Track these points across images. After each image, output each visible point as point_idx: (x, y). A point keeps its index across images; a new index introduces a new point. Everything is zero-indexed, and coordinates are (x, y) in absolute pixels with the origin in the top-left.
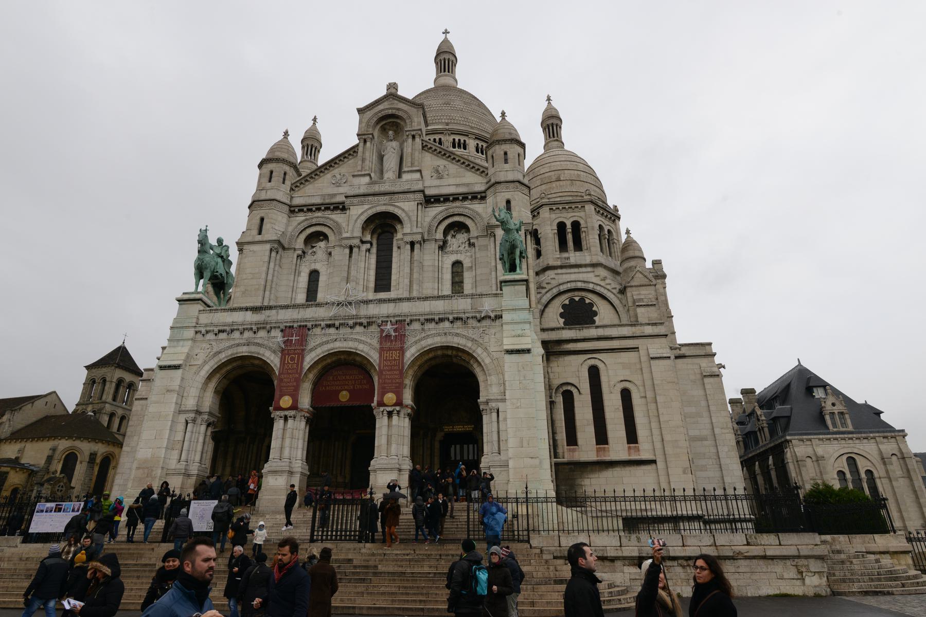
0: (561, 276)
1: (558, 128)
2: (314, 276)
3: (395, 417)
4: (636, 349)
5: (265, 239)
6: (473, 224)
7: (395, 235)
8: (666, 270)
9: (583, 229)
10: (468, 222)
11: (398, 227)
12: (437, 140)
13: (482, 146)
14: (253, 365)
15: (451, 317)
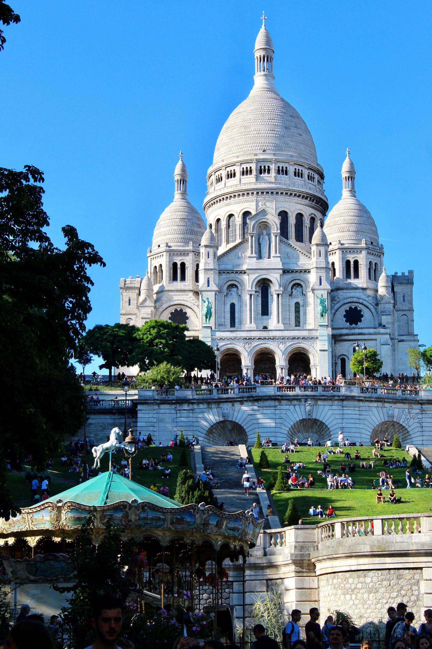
0: (345, 294)
1: (353, 180)
2: (233, 306)
3: (283, 370)
4: (375, 340)
5: (212, 289)
6: (304, 285)
7: (269, 288)
8: (415, 280)
9: (359, 266)
10: (302, 284)
11: (271, 285)
12: (267, 168)
13: (299, 170)
14: (232, 351)
15: (301, 338)
